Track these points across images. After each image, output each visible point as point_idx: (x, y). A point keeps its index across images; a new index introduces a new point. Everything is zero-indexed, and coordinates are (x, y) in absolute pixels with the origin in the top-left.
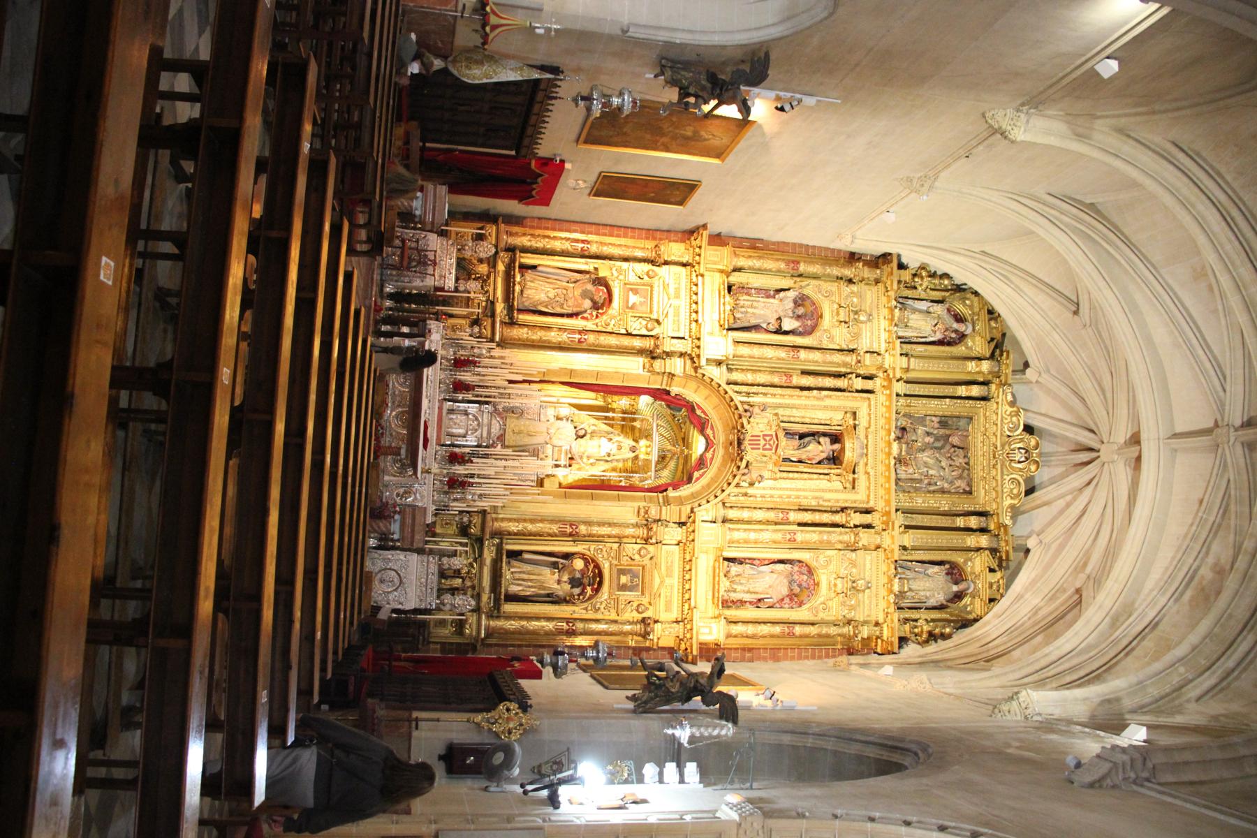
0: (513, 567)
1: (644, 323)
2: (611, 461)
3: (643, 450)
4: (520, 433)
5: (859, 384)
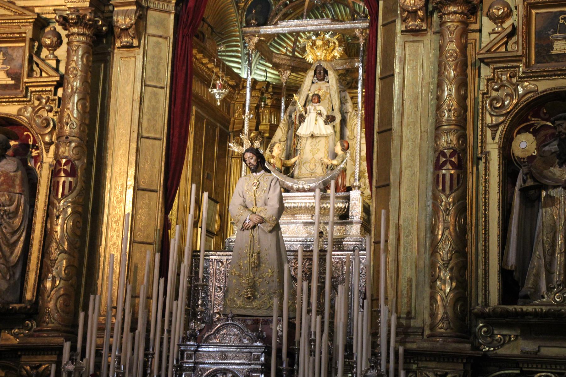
0: (536, 287)
1: (45, 52)
2: (343, 114)
3: (320, 54)
4: (253, 287)
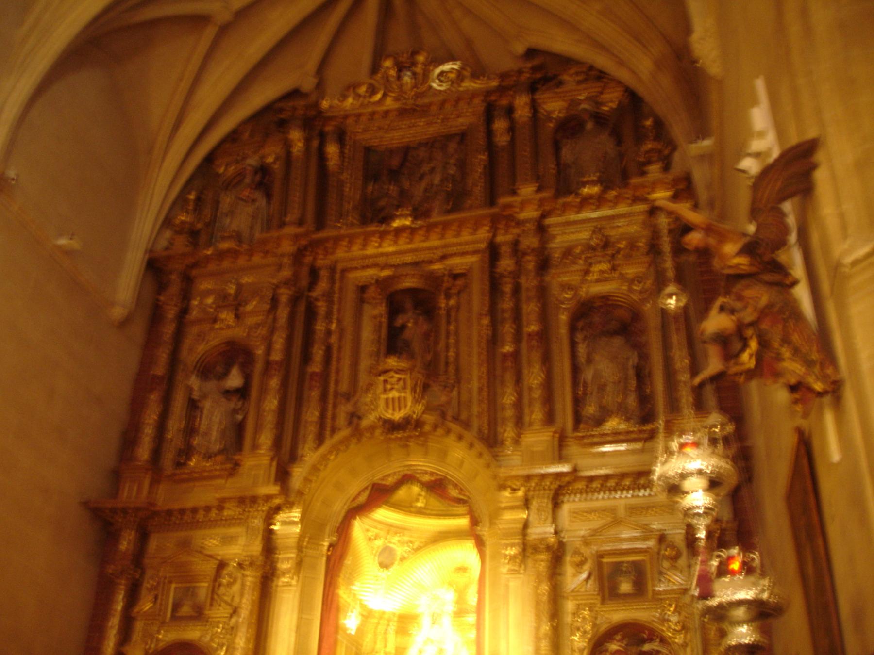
1: (222, 590)
5: (323, 285)
